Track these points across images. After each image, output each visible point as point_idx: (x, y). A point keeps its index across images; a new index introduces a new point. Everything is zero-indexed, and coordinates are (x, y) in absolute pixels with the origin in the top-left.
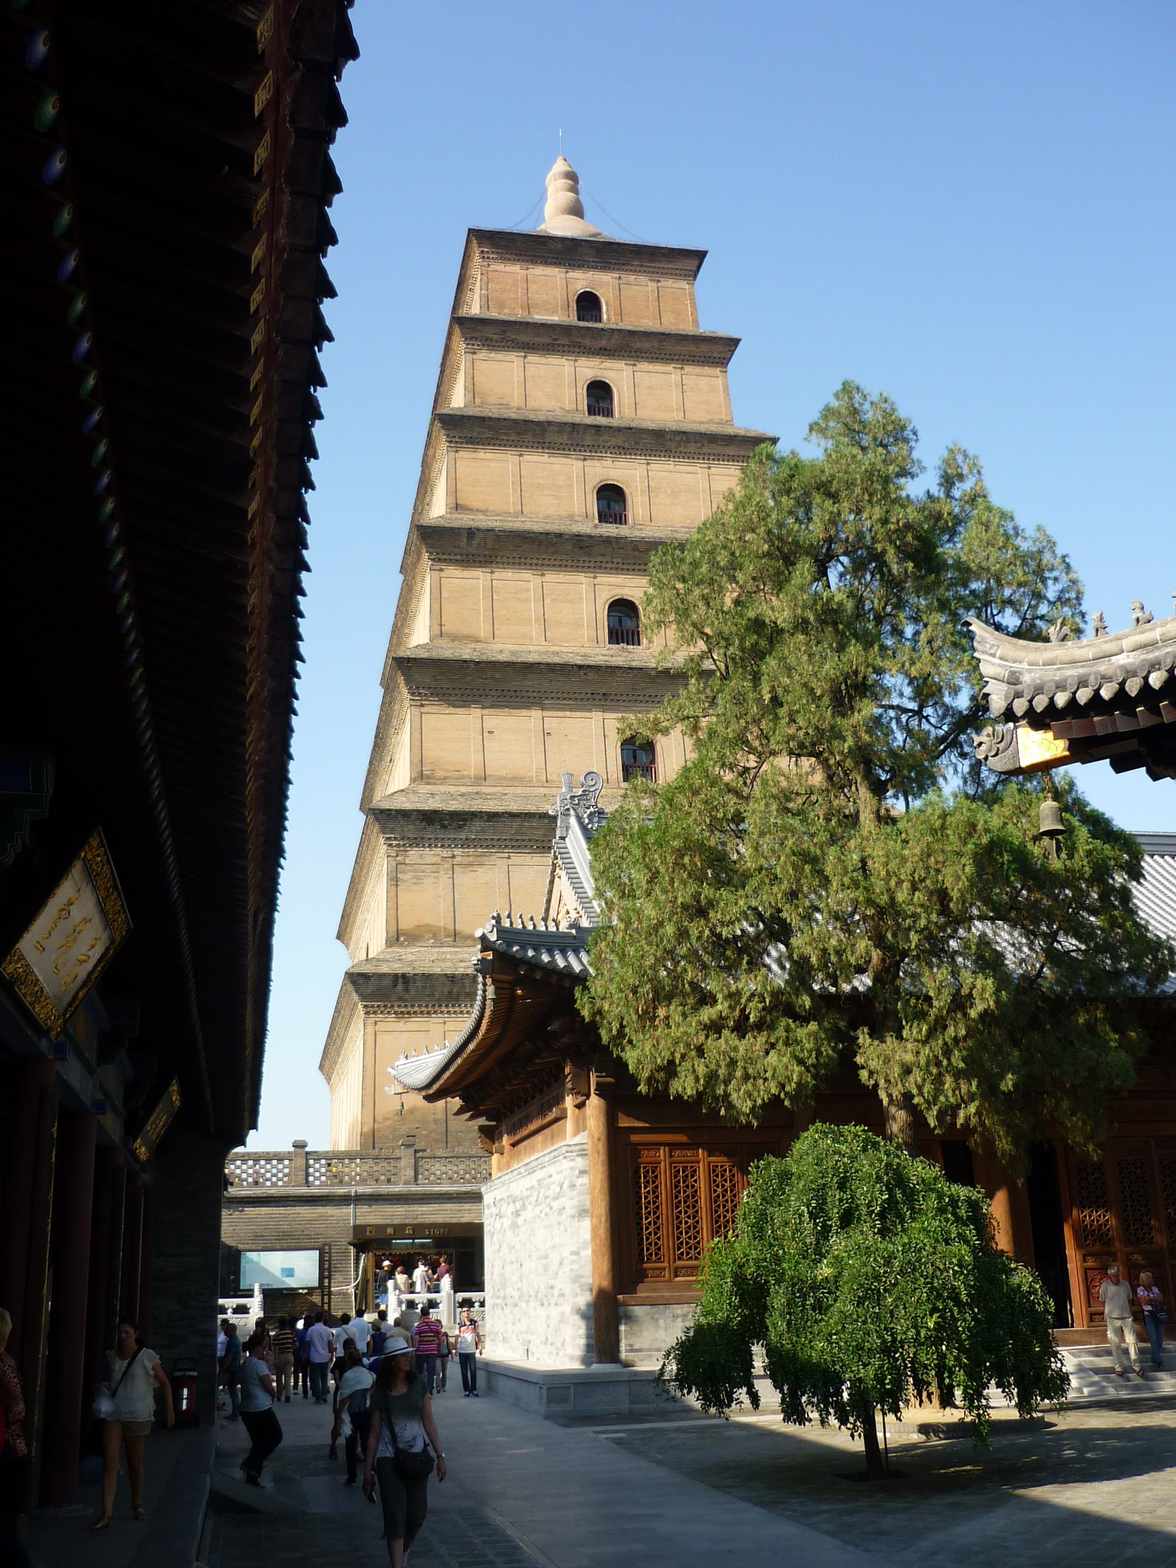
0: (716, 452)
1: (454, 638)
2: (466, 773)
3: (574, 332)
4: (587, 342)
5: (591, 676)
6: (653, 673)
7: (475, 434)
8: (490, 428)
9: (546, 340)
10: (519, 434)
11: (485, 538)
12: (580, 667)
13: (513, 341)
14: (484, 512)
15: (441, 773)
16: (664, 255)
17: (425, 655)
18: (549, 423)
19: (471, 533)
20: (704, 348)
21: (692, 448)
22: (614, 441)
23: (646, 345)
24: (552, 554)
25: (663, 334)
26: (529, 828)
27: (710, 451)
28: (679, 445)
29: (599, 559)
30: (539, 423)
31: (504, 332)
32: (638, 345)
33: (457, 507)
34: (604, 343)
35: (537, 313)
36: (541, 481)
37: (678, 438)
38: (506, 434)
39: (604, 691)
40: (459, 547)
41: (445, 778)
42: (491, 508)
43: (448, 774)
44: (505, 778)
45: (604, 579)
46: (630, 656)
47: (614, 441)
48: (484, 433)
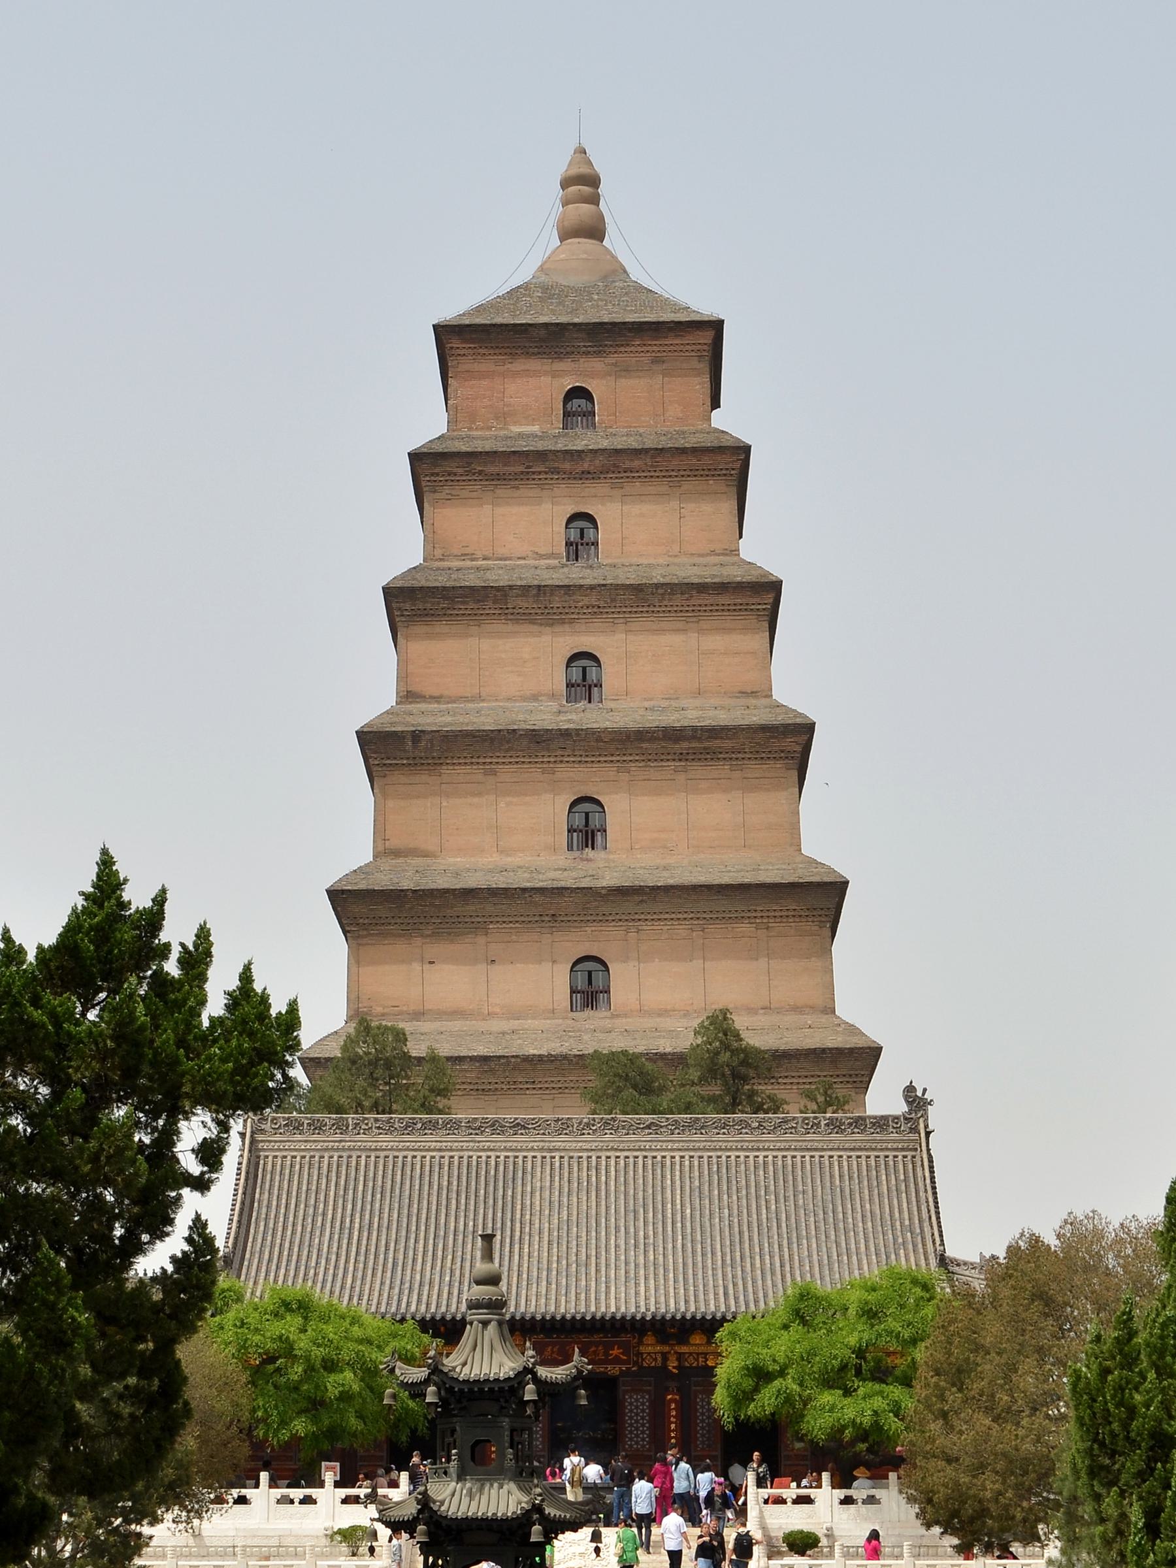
0: (707, 602)
1: (396, 853)
2: (405, 1008)
3: (551, 457)
4: (567, 466)
5: (537, 898)
6: (603, 892)
7: (429, 606)
8: (444, 598)
9: (522, 468)
10: (479, 601)
11: (431, 741)
12: (524, 890)
13: (480, 472)
14: (437, 699)
15: (379, 1010)
16: (671, 329)
17: (362, 886)
18: (511, 587)
19: (416, 736)
20: (707, 460)
21: (678, 600)
22: (586, 601)
23: (637, 463)
24: (507, 751)
25: (657, 449)
26: (462, 1070)
27: (700, 602)
28: (663, 599)
29: (560, 752)
30: (498, 589)
31: (470, 464)
32: (628, 464)
33: (407, 695)
34: (586, 466)
35: (515, 423)
36: (503, 656)
37: (660, 591)
38: (463, 603)
39: (552, 912)
40: (405, 751)
41: (383, 1015)
42: (446, 693)
43: (386, 1010)
44: (445, 1013)
45: (564, 772)
46: (592, 865)
47: (586, 601)
48: (439, 603)
